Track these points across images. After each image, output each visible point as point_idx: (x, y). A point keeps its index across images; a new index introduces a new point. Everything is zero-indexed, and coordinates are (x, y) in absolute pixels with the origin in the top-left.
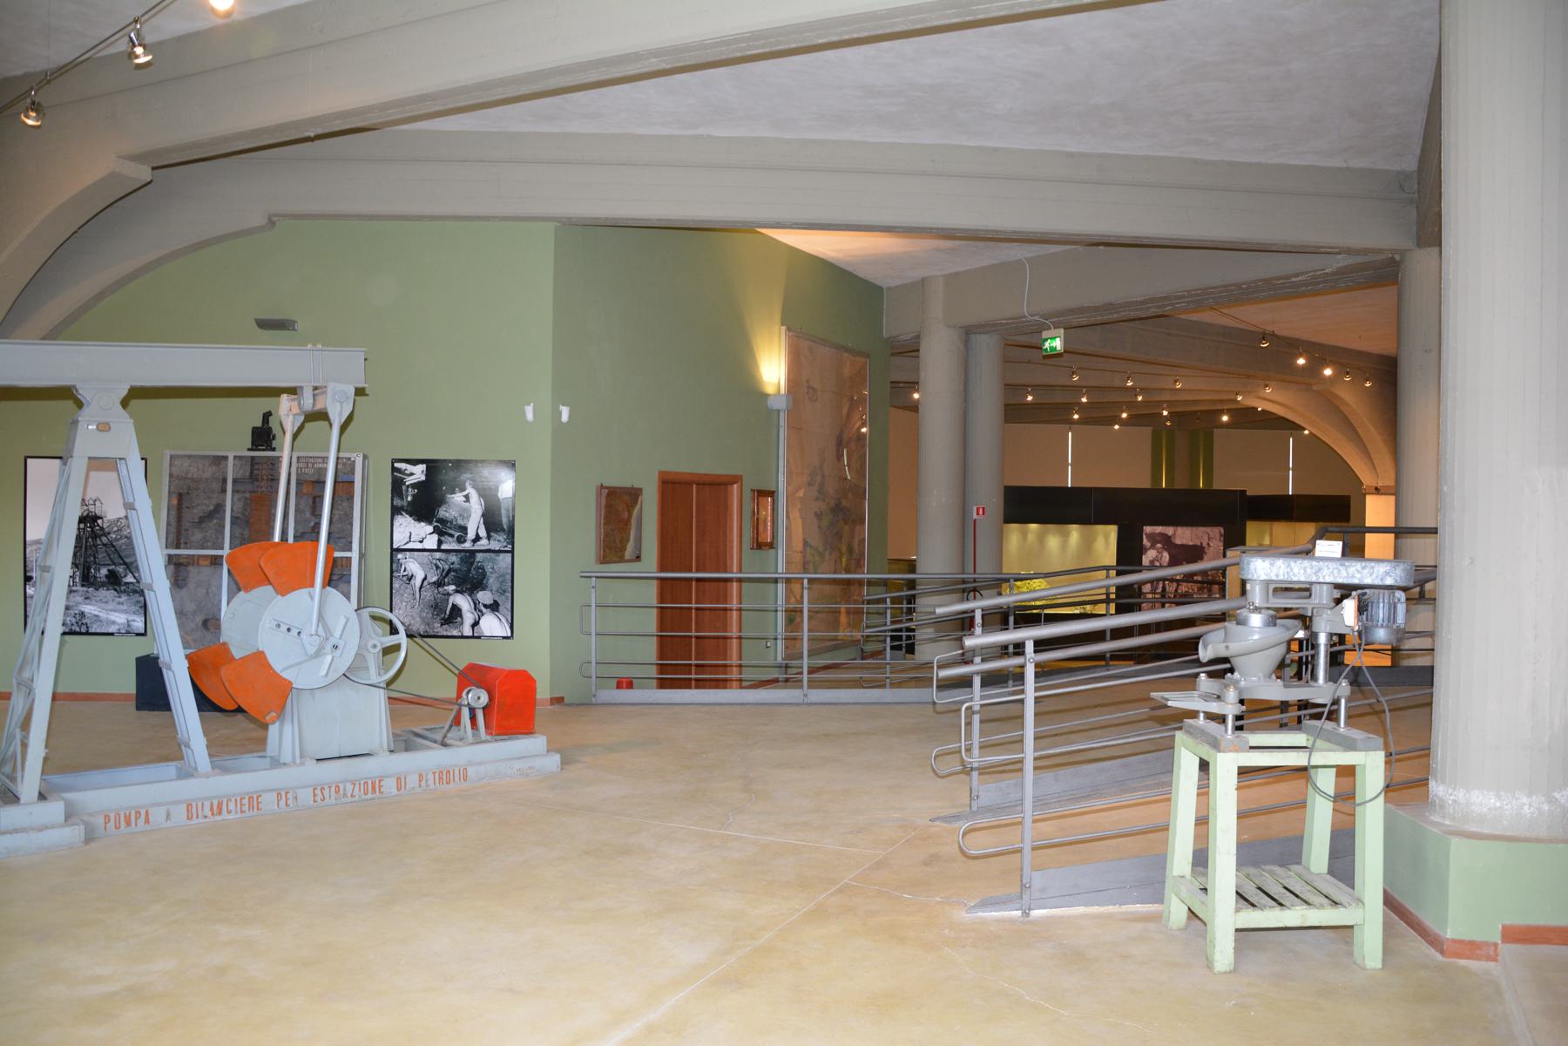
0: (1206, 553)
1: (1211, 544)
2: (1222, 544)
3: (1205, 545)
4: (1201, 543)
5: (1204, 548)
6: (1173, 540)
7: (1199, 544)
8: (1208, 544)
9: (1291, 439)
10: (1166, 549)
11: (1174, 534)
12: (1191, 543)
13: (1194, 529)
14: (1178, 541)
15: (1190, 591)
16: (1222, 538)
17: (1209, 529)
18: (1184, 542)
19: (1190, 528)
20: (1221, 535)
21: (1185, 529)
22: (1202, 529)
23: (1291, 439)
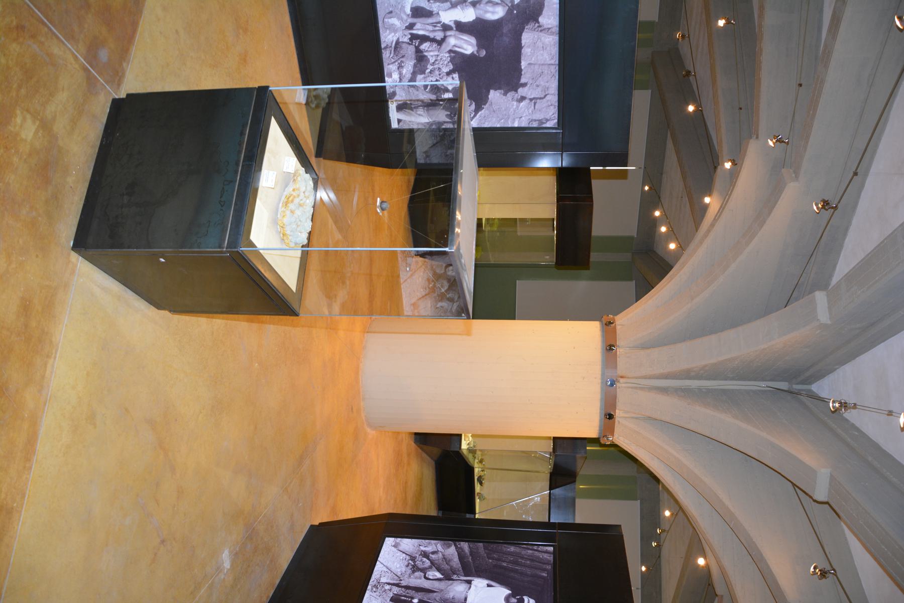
0: (505, 94)
1: (523, 104)
2: (523, 125)
3: (522, 91)
4: (524, 85)
5: (516, 91)
6: (531, 25)
7: (523, 80)
8: (523, 98)
9: (634, 168)
10: (509, 12)
11: (542, 29)
12: (524, 64)
13: (555, 70)
14: (527, 37)
15: (430, 67)
16: (535, 125)
17: (553, 98)
18: (526, 51)
19: (556, 60)
20: (541, 122)
21: (555, 50)
22: (553, 86)
23: (634, 168)
